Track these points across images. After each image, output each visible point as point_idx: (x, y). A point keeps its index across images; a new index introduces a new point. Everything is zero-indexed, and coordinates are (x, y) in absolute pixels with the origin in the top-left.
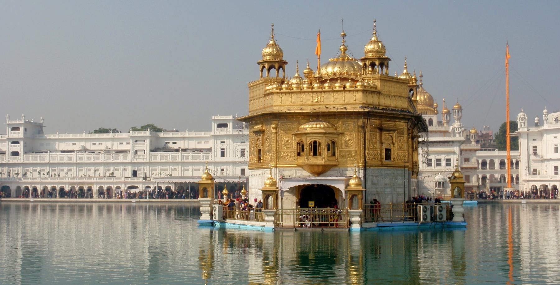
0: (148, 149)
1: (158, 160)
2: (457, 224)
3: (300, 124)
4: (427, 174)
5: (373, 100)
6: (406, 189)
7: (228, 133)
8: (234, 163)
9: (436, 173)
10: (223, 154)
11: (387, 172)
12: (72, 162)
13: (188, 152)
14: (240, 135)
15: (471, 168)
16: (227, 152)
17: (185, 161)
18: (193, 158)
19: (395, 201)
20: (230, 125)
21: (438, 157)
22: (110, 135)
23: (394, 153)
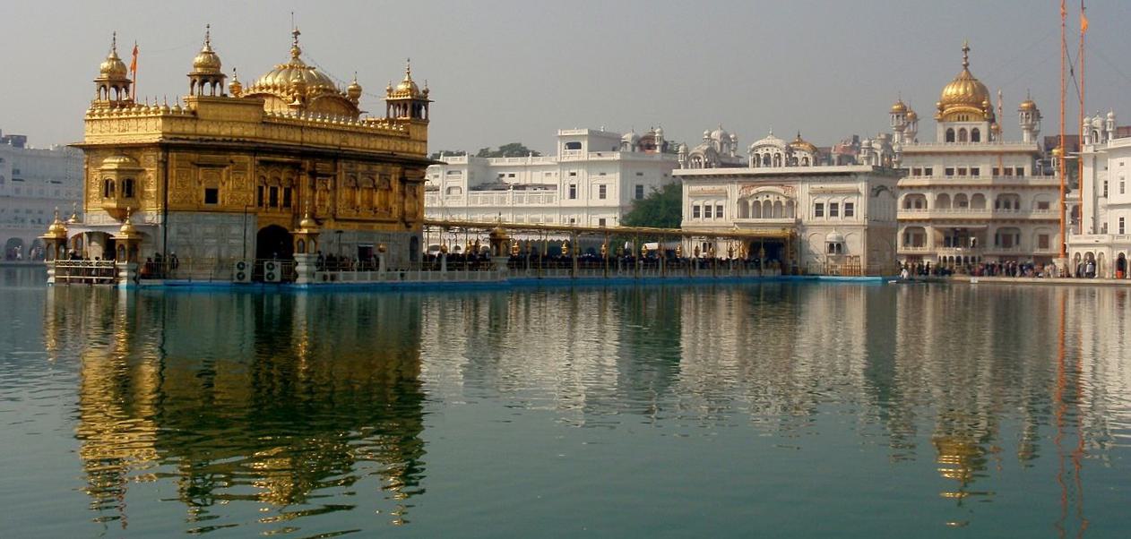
0: (465, 188)
1: (479, 205)
2: (298, 287)
3: (107, 157)
4: (815, 230)
5: (178, 128)
6: (248, 241)
7: (581, 159)
8: (589, 209)
9: (827, 227)
10: (573, 194)
11: (211, 218)
12: (506, 205)
13: (529, 190)
14: (598, 161)
15: (1050, 222)
16: (580, 191)
17: (518, 205)
18: (530, 201)
19: (223, 255)
20: (585, 144)
21: (834, 200)
22: (529, 160)
23: (223, 196)
